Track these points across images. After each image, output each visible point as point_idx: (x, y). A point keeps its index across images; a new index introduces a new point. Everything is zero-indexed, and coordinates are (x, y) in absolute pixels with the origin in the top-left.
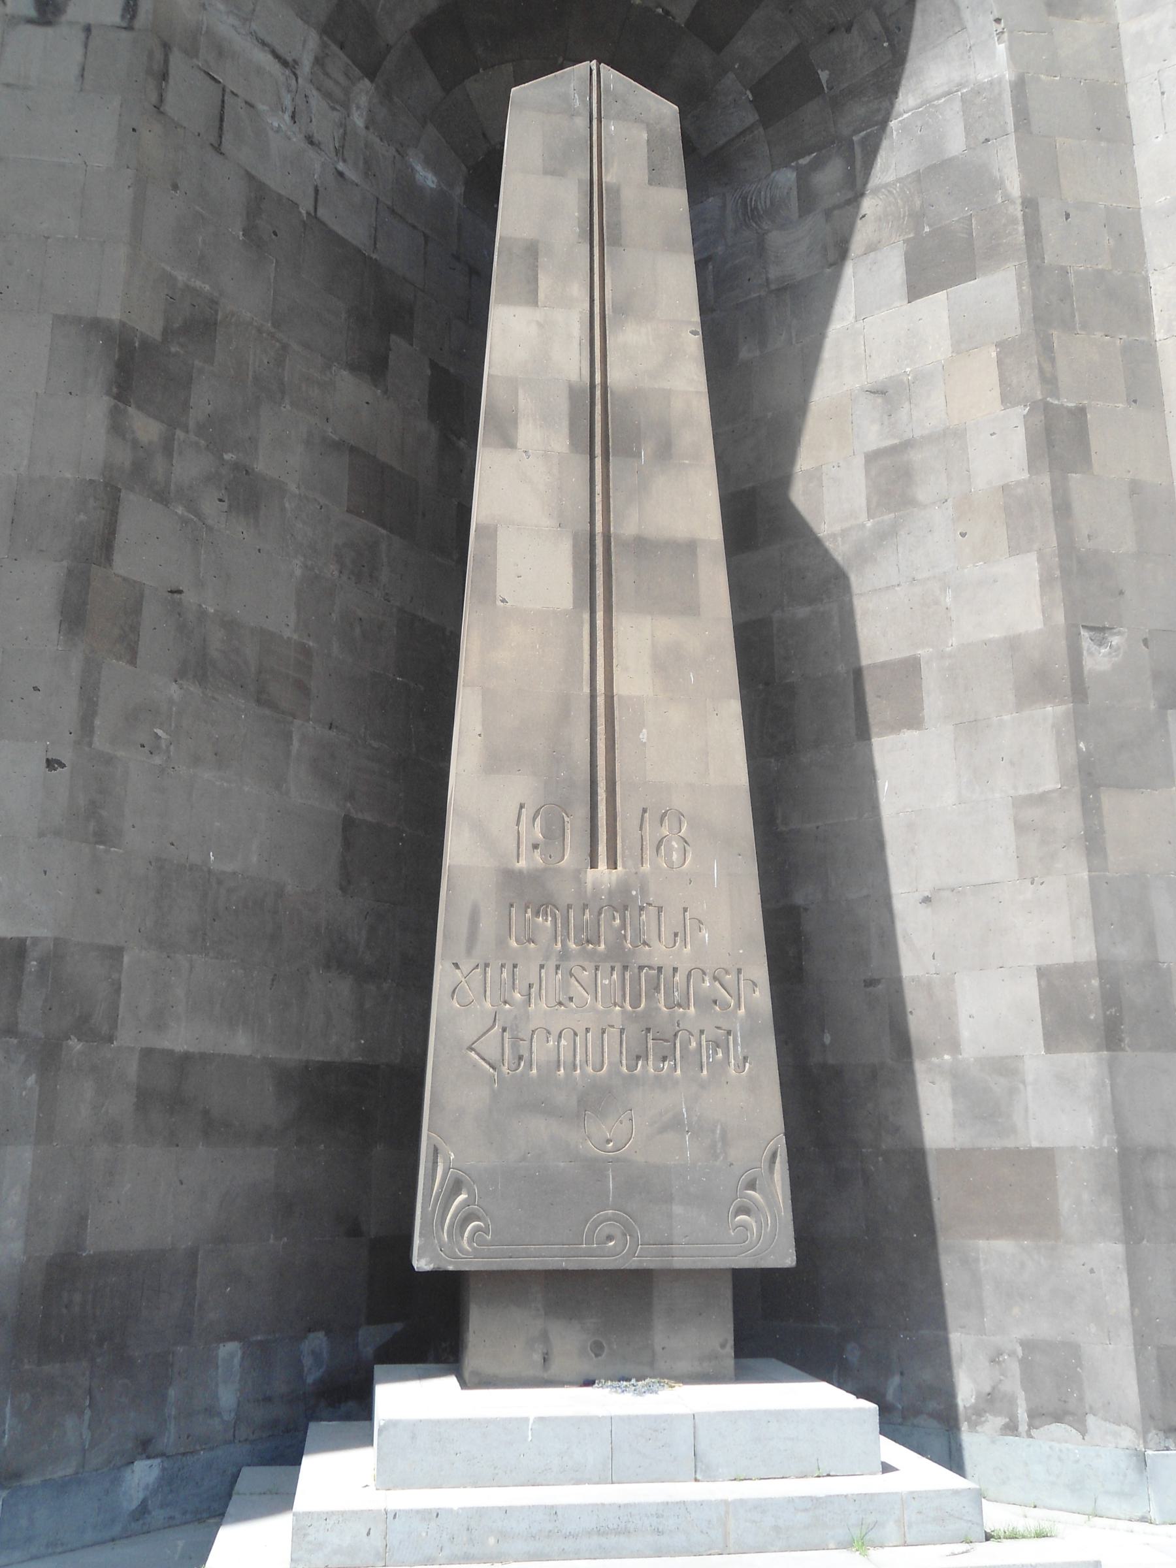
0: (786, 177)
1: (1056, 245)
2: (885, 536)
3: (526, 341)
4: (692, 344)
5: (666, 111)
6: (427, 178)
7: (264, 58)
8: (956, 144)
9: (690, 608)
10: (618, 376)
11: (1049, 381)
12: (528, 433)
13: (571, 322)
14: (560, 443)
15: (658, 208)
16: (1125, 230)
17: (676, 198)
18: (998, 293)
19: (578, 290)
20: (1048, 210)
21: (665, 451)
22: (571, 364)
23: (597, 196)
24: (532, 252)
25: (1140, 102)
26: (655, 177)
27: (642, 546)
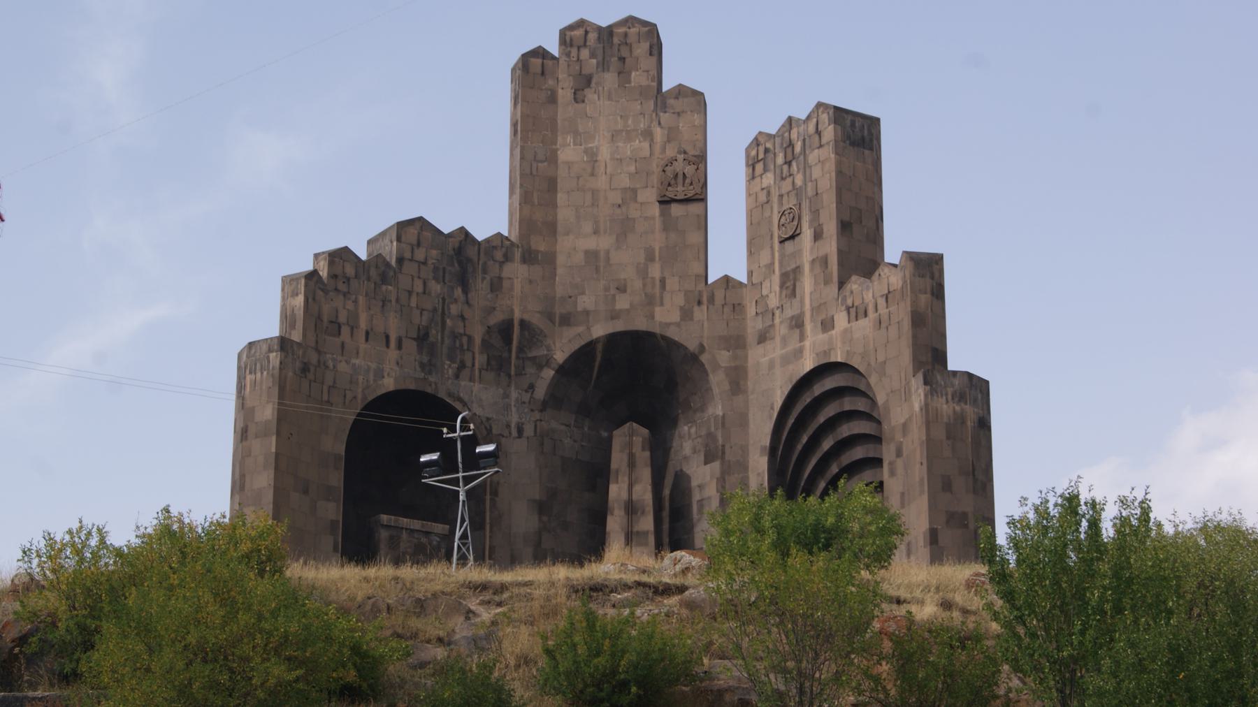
0: (686, 428)
1: (727, 457)
2: (699, 520)
3: (617, 491)
4: (649, 488)
5: (645, 432)
6: (605, 434)
7: (563, 427)
8: (713, 429)
9: (646, 544)
10: (634, 497)
11: (723, 487)
12: (616, 512)
13: (625, 486)
14: (622, 513)
15: (643, 456)
16: (745, 450)
17: (647, 454)
18: (716, 466)
19: (626, 479)
20: (727, 447)
21: (643, 513)
22: (625, 495)
23: (631, 457)
24: (617, 472)
25: (751, 416)
26: (643, 449)
27: (638, 532)
